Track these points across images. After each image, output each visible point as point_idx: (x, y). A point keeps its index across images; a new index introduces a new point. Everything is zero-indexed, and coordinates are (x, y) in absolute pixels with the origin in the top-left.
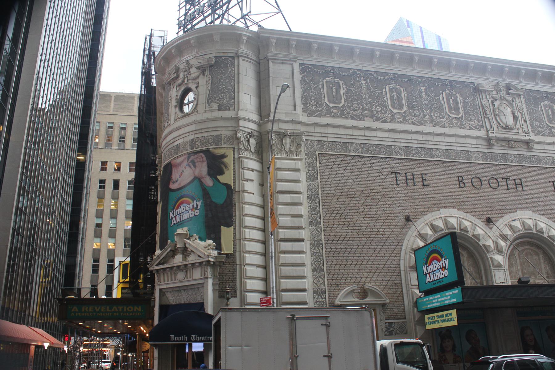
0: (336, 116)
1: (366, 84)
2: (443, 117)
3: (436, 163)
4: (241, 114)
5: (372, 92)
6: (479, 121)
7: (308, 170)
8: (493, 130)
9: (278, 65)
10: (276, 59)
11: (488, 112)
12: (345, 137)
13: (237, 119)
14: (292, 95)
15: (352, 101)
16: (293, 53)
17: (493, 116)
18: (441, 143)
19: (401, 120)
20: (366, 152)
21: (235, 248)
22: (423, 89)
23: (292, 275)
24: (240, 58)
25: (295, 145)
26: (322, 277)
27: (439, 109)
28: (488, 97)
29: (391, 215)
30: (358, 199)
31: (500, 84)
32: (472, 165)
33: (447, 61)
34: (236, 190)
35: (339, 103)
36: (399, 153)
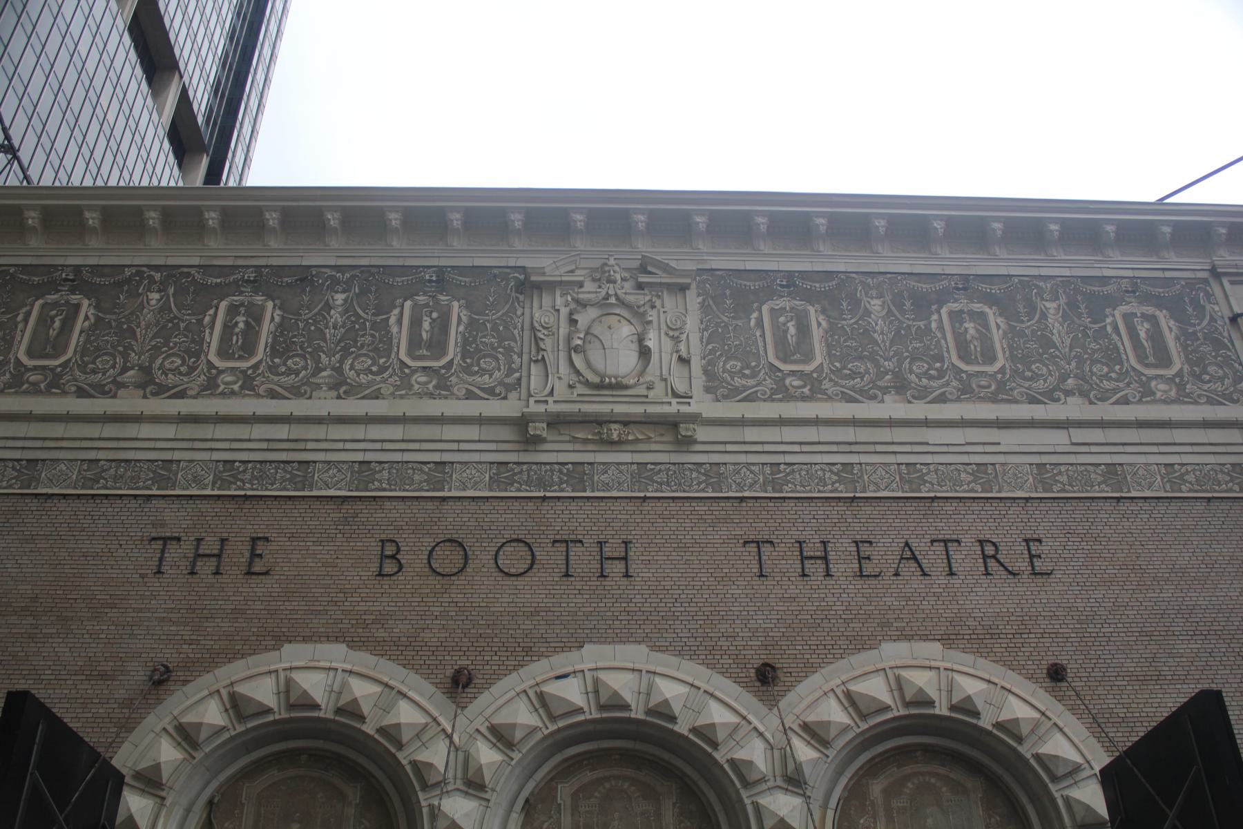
0: (35, 391)
1: (159, 301)
2: (383, 369)
3: (317, 505)
5: (171, 321)
6: (510, 372)
8: (551, 393)
11: (548, 344)
12: (39, 444)
15: (98, 349)
17: (562, 355)
19: (236, 387)
22: (340, 298)
27: (376, 349)
30: (13, 619)
31: (612, 262)
33: (425, 213)
35: (56, 357)
36: (197, 480)
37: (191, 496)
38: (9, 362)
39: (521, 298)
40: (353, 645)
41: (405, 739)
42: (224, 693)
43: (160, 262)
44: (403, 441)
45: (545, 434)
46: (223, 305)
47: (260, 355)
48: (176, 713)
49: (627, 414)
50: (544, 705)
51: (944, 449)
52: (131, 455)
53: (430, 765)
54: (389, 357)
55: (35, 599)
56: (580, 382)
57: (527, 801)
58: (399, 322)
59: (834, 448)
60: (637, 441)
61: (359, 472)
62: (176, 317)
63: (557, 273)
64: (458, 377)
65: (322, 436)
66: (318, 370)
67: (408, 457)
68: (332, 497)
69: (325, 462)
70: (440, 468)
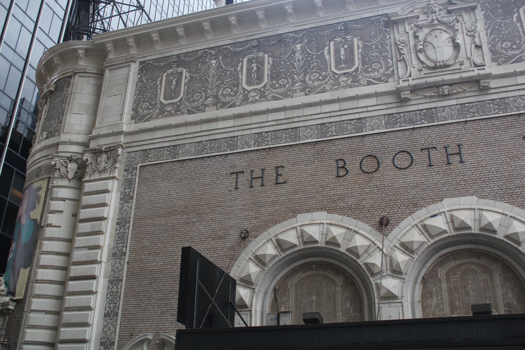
0: (170, 114)
1: (216, 63)
2: (325, 77)
3: (303, 147)
4: (64, 137)
5: (223, 72)
6: (388, 68)
7: (125, 189)
8: (410, 75)
9: (115, 71)
10: (112, 66)
11: (405, 51)
13: (57, 145)
14: (122, 103)
15: (193, 91)
16: (133, 52)
17: (413, 55)
18: (314, 117)
19: (257, 98)
20: (200, 152)
21: (26, 292)
22: (299, 46)
23: (73, 321)
24: (77, 76)
25: (111, 161)
26: (115, 323)
27: (320, 69)
28: (408, 28)
29: (221, 233)
30: (179, 217)
32: (366, 139)
34: (42, 225)
35: (176, 98)
36: (247, 144)
37: (245, 152)
38: (157, 103)
39: (388, 30)
40: (329, 211)
41: (360, 253)
42: (274, 239)
44: (340, 111)
45: (410, 97)
46: (245, 60)
47: (266, 80)
48: (254, 251)
49: (451, 80)
50: (427, 230)
52: (216, 137)
53: (374, 264)
54: (327, 71)
55: (186, 207)
56: (424, 67)
57: (423, 278)
58: (329, 53)
60: (458, 93)
61: (321, 129)
62: (225, 70)
63: (405, 13)
64: (362, 75)
65: (301, 114)
66: (294, 83)
67: (343, 118)
69: (304, 126)
70: (360, 121)
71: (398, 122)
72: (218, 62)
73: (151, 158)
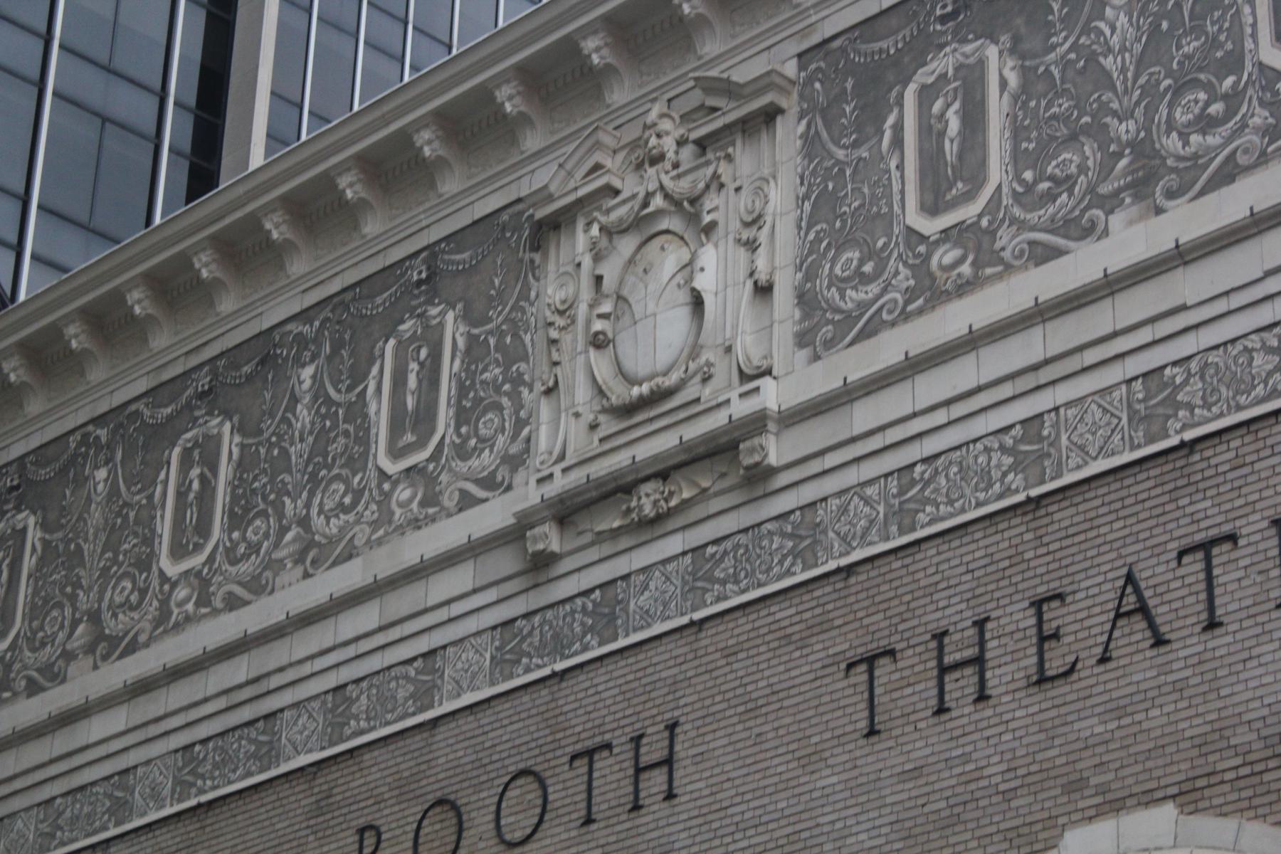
3: (284, 789)
8: (562, 457)
19: (190, 607)
32: (443, 732)
43: (103, 407)
44: (381, 629)
45: (555, 547)
49: (656, 458)
51: (1220, 307)
59: (1006, 390)
63: (572, 185)
68: (301, 769)
71: (927, 501)
72: (112, 472)
73: (1191, 407)
